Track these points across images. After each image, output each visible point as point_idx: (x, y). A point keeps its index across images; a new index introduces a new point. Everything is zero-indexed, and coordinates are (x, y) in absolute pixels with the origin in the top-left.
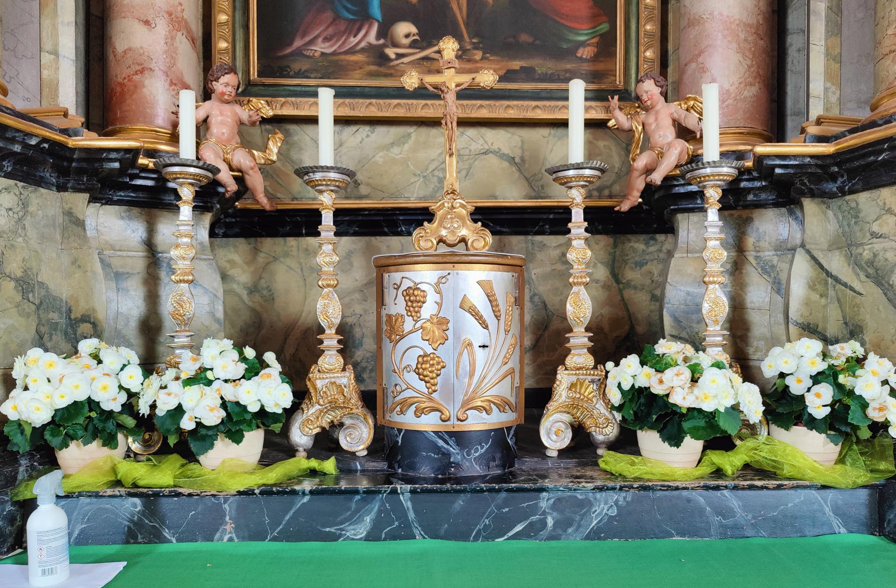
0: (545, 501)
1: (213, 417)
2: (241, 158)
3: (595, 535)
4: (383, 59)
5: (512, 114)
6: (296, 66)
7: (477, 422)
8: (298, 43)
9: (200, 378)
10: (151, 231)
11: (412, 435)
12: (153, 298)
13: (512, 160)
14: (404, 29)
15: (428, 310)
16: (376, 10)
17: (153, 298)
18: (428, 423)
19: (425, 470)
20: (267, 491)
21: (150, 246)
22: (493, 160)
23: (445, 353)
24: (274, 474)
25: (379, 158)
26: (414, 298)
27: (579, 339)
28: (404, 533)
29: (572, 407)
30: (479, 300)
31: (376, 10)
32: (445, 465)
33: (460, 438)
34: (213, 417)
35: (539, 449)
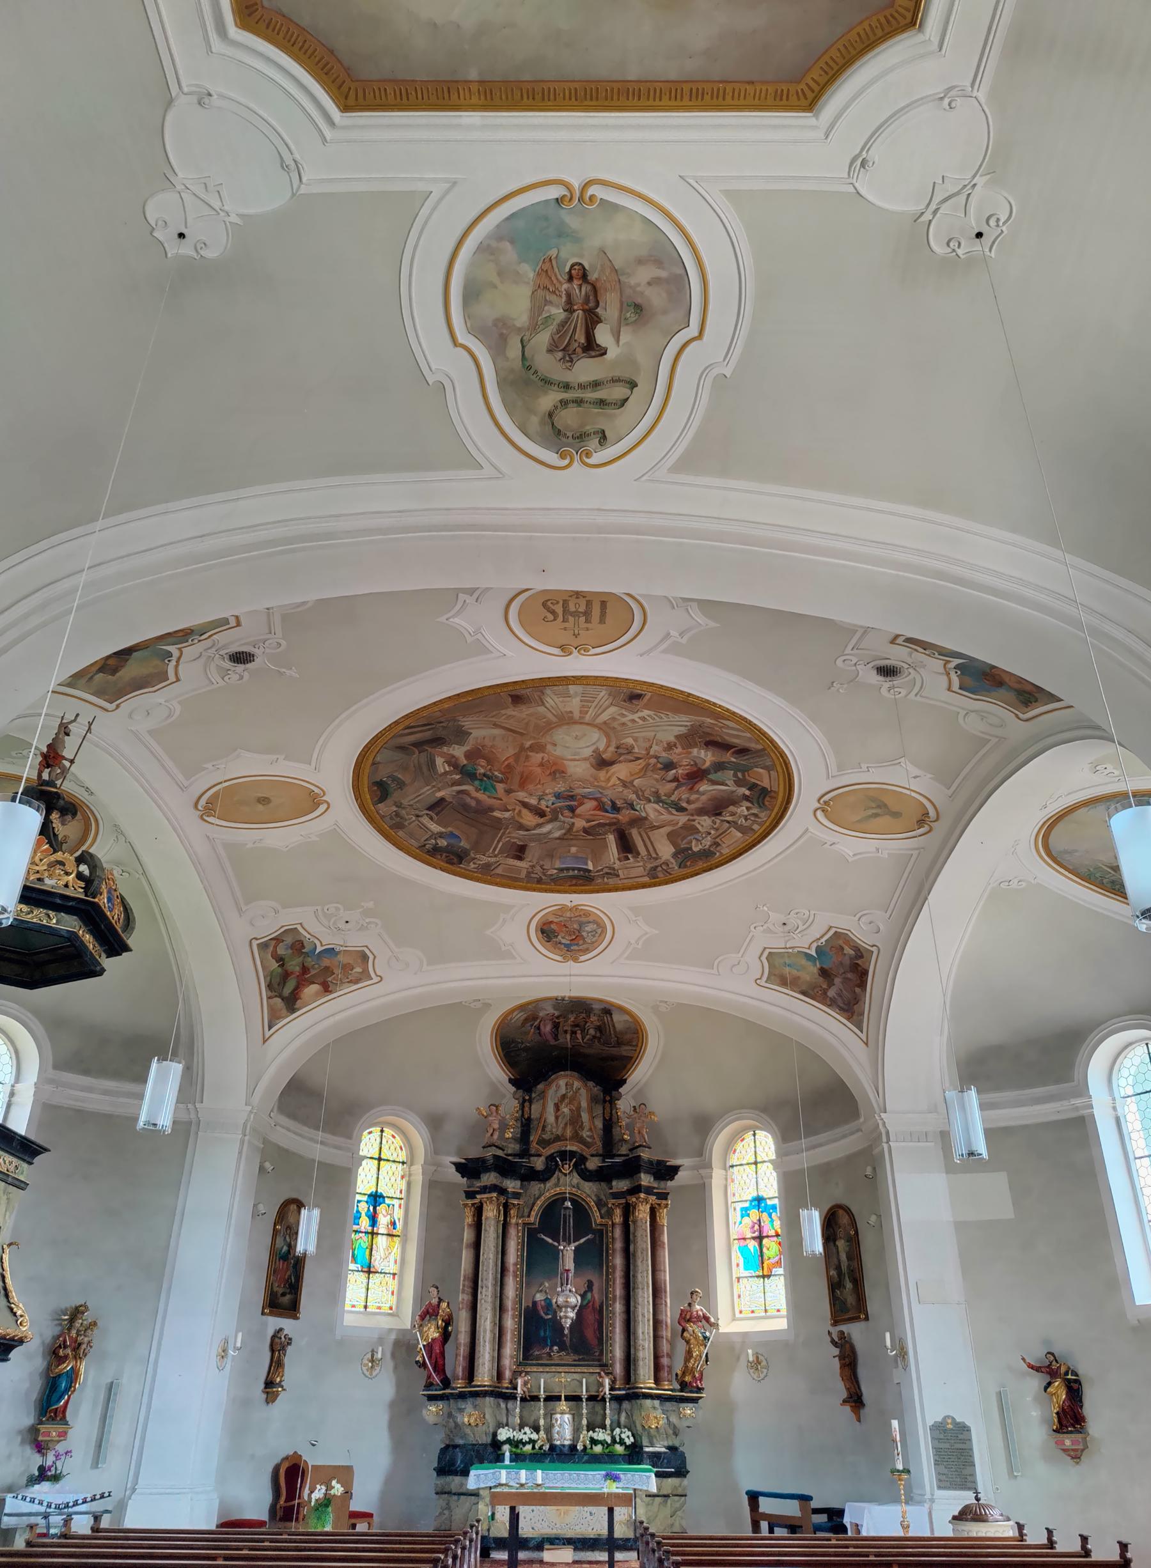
0: (576, 1457)
1: (528, 1440)
2: (525, 1389)
3: (584, 1463)
4: (551, 1356)
5: (579, 1370)
6: (531, 1358)
7: (567, 1443)
8: (531, 1352)
9: (525, 1433)
10: (507, 1405)
11: (556, 1446)
12: (507, 1420)
13: (578, 1381)
14: (555, 1348)
15: (559, 1422)
16: (549, 1344)
17: (507, 1420)
18: (558, 1443)
19: (558, 1452)
20: (534, 1454)
21: (507, 1407)
22: (575, 1381)
23: (561, 1430)
24: (535, 1451)
25: (549, 1381)
26: (557, 1420)
27: (585, 1428)
28: (553, 1462)
29: (583, 1441)
30: (567, 1420)
31: (549, 1344)
32: (561, 1450)
33: (564, 1446)
34: (528, 1440)
35: (577, 1450)
